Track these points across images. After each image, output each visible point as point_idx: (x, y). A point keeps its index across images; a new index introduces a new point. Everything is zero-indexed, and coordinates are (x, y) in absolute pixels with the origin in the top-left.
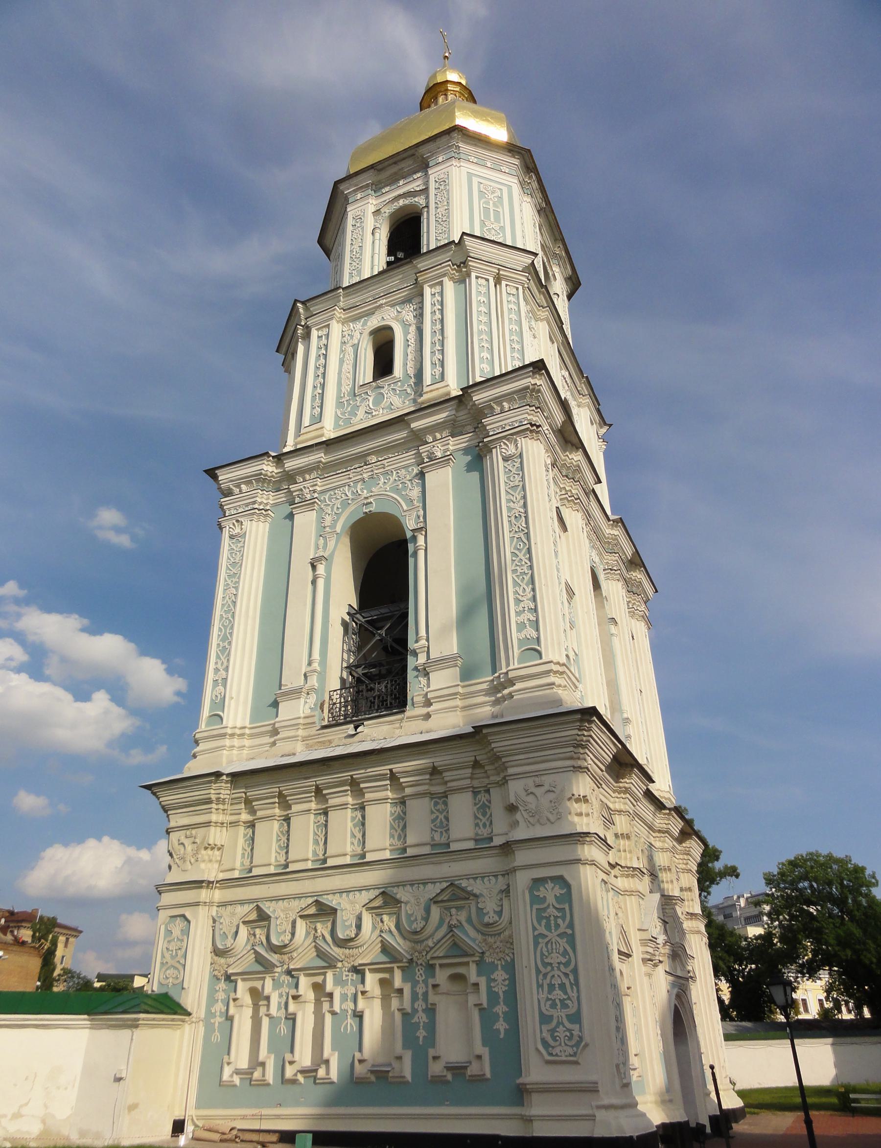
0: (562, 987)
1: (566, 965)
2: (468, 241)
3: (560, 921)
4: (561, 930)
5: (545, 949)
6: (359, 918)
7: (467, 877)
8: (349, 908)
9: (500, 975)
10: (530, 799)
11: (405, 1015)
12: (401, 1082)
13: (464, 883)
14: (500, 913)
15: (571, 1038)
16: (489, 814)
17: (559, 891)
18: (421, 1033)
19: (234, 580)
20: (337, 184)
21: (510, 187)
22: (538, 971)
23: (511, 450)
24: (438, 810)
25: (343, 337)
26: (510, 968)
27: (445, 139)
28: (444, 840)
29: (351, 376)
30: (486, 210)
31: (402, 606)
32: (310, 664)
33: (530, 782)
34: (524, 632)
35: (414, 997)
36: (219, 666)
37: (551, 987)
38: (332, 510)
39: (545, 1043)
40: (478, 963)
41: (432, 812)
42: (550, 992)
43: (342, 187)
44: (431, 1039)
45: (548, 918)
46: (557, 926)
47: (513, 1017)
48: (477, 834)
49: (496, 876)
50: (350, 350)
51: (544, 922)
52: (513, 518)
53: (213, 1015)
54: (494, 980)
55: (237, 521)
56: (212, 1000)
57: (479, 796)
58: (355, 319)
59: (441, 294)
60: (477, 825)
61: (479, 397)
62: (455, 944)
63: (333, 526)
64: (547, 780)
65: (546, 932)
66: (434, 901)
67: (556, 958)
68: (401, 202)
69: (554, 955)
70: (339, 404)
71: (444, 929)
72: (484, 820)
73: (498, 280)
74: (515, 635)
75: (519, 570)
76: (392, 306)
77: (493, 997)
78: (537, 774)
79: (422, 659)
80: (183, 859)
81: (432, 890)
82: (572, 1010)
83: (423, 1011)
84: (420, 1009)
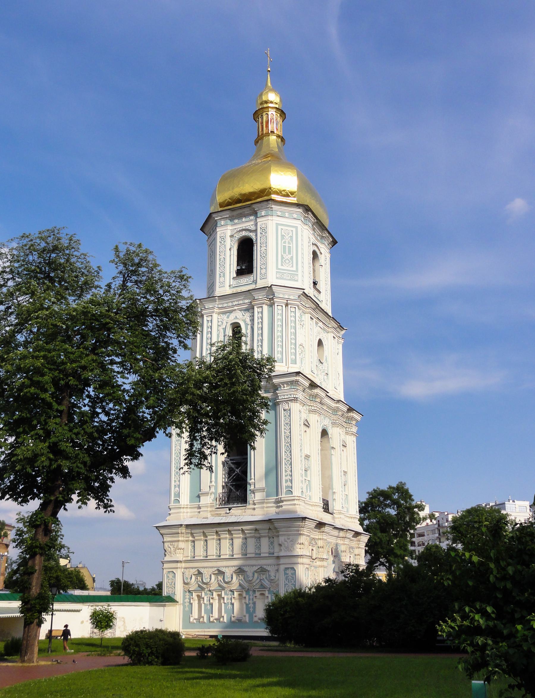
6: (232, 575)
7: (266, 565)
8: (228, 572)
10: (286, 543)
11: (247, 605)
12: (245, 622)
13: (265, 567)
14: (275, 577)
18: (251, 610)
20: (211, 214)
21: (296, 228)
23: (287, 407)
25: (218, 322)
27: (265, 203)
28: (259, 552)
30: (284, 247)
31: (245, 457)
32: (211, 482)
33: (286, 537)
35: (249, 599)
40: (269, 591)
43: (214, 216)
44: (254, 611)
46: (291, 582)
53: (186, 603)
56: (184, 598)
59: (262, 313)
62: (262, 585)
64: (291, 537)
68: (244, 234)
71: (258, 580)
73: (287, 305)
74: (284, 484)
76: (240, 310)
78: (289, 535)
79: (252, 487)
80: (170, 552)
81: (255, 568)
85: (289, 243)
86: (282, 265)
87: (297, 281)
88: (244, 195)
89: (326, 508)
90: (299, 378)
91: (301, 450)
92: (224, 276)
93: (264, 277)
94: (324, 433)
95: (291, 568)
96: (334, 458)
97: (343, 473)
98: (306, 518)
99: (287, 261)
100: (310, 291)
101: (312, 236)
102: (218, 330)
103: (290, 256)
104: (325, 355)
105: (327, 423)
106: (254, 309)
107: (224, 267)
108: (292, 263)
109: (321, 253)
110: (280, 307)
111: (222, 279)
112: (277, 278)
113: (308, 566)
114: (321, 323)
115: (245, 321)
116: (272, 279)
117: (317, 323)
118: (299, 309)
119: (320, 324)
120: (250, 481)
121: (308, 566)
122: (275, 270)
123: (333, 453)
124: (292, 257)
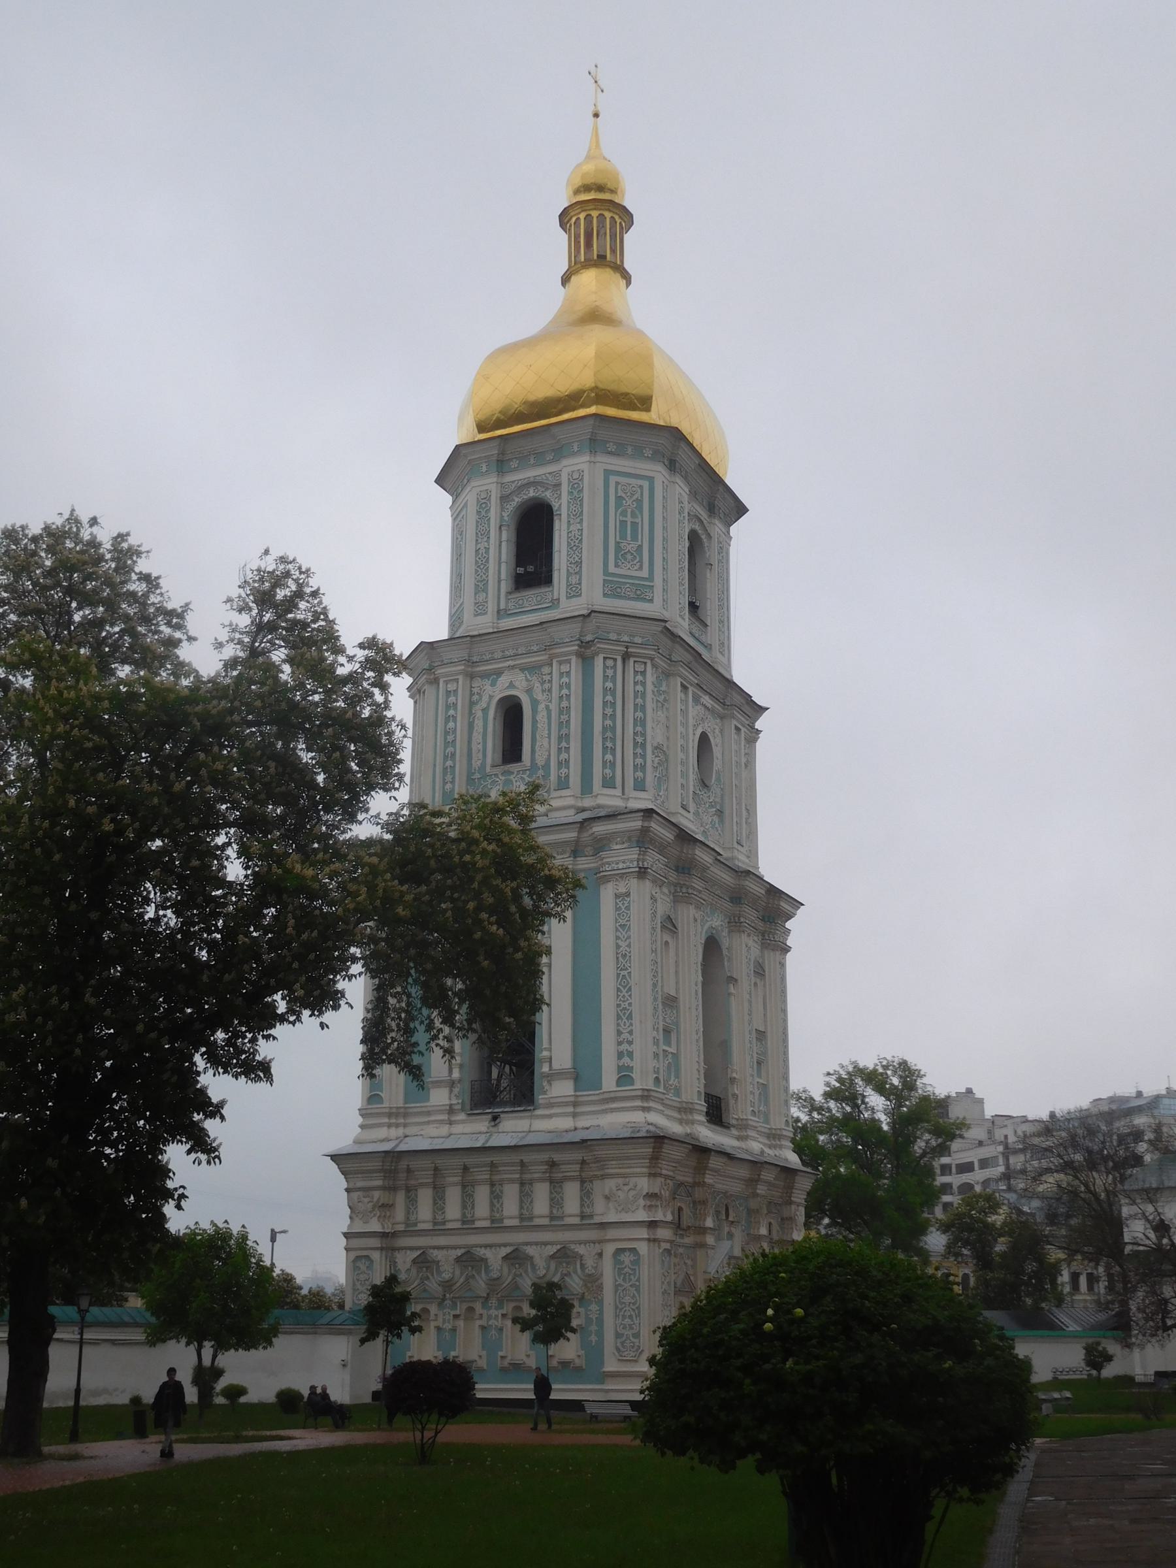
21: (651, 480)
22: (616, 1307)
26: (600, 1303)
29: (480, 747)
33: (620, 1181)
39: (618, 1349)
46: (630, 1280)
47: (600, 1334)
48: (582, 1212)
50: (479, 714)
58: (485, 675)
60: (582, 1206)
61: (599, 829)
64: (633, 1180)
66: (552, 1257)
67: (627, 1299)
68: (532, 493)
73: (626, 657)
76: (522, 670)
78: (624, 1176)
82: (634, 1331)
85: (633, 515)
86: (617, 566)
87: (651, 601)
88: (533, 404)
89: (716, 1113)
90: (655, 826)
91: (655, 985)
92: (485, 590)
93: (574, 591)
94: (712, 946)
95: (631, 1250)
96: (733, 1002)
97: (754, 1034)
98: (664, 1137)
99: (629, 557)
100: (683, 625)
101: (686, 498)
103: (632, 546)
104: (715, 768)
105: (718, 923)
107: (487, 570)
108: (641, 561)
109: (709, 536)
110: (610, 663)
112: (605, 595)
113: (668, 1246)
114: (707, 698)
115: (529, 691)
116: (593, 595)
117: (696, 700)
118: (654, 666)
119: (706, 700)
120: (541, 1053)
121: (668, 1246)
122: (599, 577)
123: (732, 990)
124: (640, 548)
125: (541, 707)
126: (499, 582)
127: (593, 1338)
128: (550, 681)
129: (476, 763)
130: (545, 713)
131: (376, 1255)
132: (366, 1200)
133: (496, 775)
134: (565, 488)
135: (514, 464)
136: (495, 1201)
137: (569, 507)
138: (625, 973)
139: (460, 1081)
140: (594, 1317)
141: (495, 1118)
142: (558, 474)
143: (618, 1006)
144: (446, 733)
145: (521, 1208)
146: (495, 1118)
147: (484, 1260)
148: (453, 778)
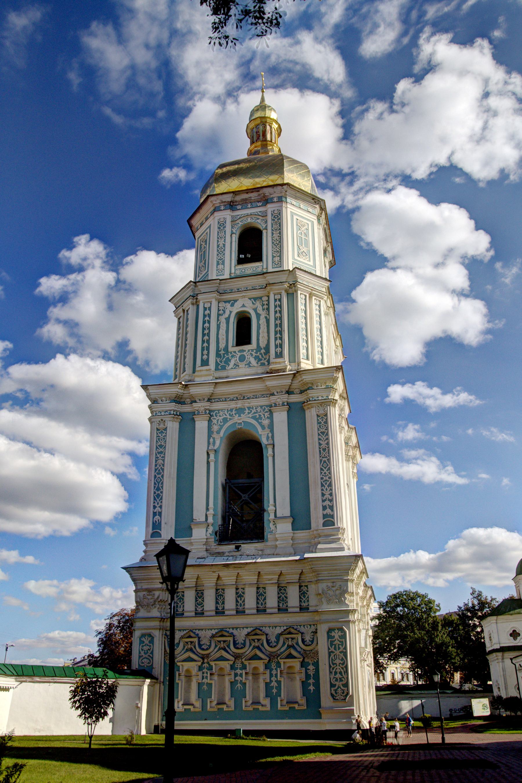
0: (340, 673)
1: (343, 664)
2: (298, 273)
3: (340, 646)
4: (341, 650)
5: (333, 658)
9: (311, 667)
10: (329, 592)
14: (312, 642)
15: (343, 693)
16: (307, 597)
17: (340, 634)
18: (274, 691)
19: (162, 455)
22: (330, 666)
24: (281, 593)
26: (316, 665)
28: (284, 606)
34: (326, 511)
35: (271, 675)
36: (156, 504)
37: (336, 673)
38: (218, 422)
39: (332, 695)
41: (278, 594)
42: (335, 675)
45: (335, 645)
46: (339, 648)
47: (317, 685)
49: (310, 625)
51: (333, 646)
52: (321, 449)
54: (309, 669)
55: (162, 420)
57: (302, 588)
60: (300, 601)
63: (218, 432)
65: (334, 651)
66: (281, 634)
68: (249, 220)
69: (338, 660)
70: (218, 355)
72: (304, 599)
75: (324, 478)
76: (250, 299)
77: (308, 676)
82: (344, 682)
83: (275, 681)
84: (274, 680)
92: (223, 263)
102: (218, 320)
106: (268, 297)
107: (224, 254)
111: (221, 267)
115: (255, 310)
125: (262, 318)
126: (231, 260)
127: (312, 688)
128: (268, 305)
129: (222, 345)
130: (265, 320)
131: (157, 634)
132: (149, 597)
133: (235, 352)
134: (269, 218)
135: (239, 207)
136: (239, 599)
137: (272, 227)
138: (326, 459)
139: (212, 525)
140: (311, 673)
141: (237, 548)
142: (266, 212)
143: (322, 478)
144: (204, 329)
145: (258, 603)
146: (237, 548)
147: (232, 635)
148: (208, 353)
